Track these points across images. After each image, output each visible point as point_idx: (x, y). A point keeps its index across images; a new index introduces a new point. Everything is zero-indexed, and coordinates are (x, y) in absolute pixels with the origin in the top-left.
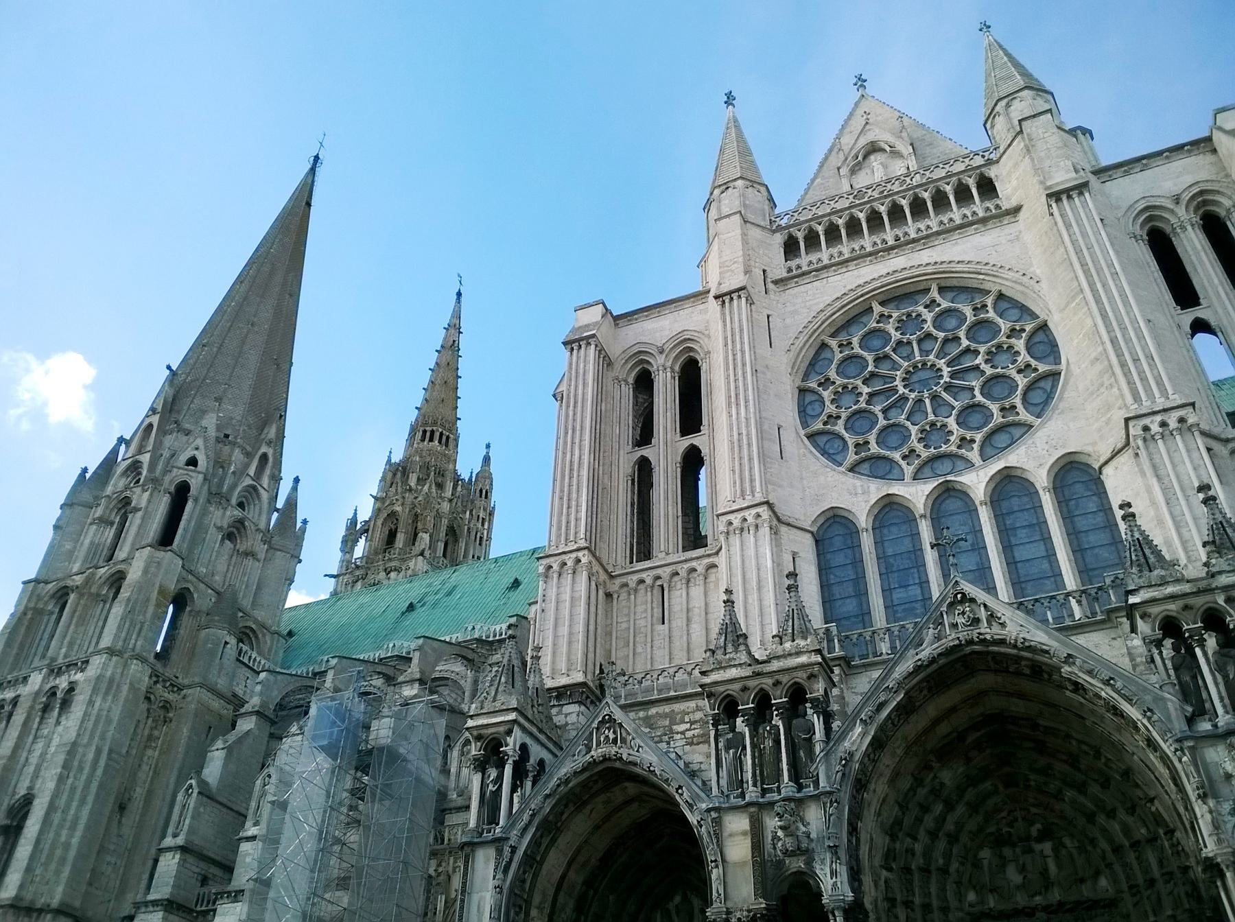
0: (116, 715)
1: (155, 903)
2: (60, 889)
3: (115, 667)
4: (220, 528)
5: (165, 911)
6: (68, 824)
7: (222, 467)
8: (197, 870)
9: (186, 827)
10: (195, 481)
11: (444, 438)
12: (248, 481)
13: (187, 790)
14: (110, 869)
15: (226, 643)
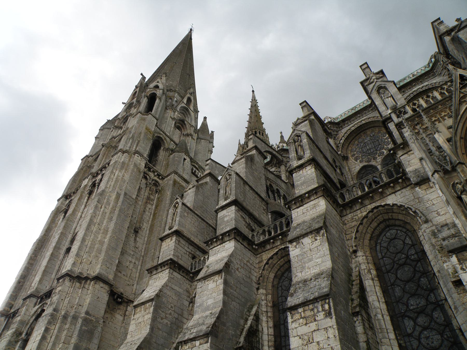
0: (127, 177)
1: (163, 265)
2: (99, 266)
3: (125, 157)
4: (173, 119)
5: (170, 268)
6: (102, 231)
7: (171, 99)
8: (188, 250)
9: (177, 222)
10: (159, 93)
11: (261, 134)
12: (183, 105)
13: (175, 206)
14: (131, 266)
15: (185, 159)
